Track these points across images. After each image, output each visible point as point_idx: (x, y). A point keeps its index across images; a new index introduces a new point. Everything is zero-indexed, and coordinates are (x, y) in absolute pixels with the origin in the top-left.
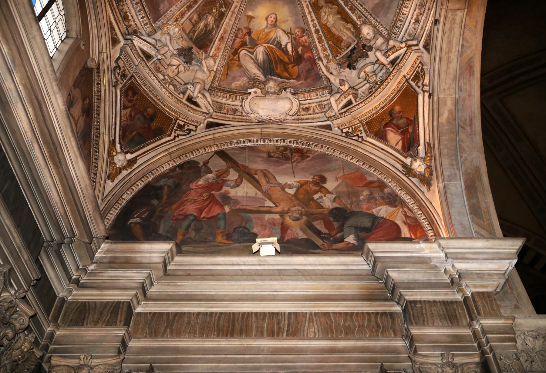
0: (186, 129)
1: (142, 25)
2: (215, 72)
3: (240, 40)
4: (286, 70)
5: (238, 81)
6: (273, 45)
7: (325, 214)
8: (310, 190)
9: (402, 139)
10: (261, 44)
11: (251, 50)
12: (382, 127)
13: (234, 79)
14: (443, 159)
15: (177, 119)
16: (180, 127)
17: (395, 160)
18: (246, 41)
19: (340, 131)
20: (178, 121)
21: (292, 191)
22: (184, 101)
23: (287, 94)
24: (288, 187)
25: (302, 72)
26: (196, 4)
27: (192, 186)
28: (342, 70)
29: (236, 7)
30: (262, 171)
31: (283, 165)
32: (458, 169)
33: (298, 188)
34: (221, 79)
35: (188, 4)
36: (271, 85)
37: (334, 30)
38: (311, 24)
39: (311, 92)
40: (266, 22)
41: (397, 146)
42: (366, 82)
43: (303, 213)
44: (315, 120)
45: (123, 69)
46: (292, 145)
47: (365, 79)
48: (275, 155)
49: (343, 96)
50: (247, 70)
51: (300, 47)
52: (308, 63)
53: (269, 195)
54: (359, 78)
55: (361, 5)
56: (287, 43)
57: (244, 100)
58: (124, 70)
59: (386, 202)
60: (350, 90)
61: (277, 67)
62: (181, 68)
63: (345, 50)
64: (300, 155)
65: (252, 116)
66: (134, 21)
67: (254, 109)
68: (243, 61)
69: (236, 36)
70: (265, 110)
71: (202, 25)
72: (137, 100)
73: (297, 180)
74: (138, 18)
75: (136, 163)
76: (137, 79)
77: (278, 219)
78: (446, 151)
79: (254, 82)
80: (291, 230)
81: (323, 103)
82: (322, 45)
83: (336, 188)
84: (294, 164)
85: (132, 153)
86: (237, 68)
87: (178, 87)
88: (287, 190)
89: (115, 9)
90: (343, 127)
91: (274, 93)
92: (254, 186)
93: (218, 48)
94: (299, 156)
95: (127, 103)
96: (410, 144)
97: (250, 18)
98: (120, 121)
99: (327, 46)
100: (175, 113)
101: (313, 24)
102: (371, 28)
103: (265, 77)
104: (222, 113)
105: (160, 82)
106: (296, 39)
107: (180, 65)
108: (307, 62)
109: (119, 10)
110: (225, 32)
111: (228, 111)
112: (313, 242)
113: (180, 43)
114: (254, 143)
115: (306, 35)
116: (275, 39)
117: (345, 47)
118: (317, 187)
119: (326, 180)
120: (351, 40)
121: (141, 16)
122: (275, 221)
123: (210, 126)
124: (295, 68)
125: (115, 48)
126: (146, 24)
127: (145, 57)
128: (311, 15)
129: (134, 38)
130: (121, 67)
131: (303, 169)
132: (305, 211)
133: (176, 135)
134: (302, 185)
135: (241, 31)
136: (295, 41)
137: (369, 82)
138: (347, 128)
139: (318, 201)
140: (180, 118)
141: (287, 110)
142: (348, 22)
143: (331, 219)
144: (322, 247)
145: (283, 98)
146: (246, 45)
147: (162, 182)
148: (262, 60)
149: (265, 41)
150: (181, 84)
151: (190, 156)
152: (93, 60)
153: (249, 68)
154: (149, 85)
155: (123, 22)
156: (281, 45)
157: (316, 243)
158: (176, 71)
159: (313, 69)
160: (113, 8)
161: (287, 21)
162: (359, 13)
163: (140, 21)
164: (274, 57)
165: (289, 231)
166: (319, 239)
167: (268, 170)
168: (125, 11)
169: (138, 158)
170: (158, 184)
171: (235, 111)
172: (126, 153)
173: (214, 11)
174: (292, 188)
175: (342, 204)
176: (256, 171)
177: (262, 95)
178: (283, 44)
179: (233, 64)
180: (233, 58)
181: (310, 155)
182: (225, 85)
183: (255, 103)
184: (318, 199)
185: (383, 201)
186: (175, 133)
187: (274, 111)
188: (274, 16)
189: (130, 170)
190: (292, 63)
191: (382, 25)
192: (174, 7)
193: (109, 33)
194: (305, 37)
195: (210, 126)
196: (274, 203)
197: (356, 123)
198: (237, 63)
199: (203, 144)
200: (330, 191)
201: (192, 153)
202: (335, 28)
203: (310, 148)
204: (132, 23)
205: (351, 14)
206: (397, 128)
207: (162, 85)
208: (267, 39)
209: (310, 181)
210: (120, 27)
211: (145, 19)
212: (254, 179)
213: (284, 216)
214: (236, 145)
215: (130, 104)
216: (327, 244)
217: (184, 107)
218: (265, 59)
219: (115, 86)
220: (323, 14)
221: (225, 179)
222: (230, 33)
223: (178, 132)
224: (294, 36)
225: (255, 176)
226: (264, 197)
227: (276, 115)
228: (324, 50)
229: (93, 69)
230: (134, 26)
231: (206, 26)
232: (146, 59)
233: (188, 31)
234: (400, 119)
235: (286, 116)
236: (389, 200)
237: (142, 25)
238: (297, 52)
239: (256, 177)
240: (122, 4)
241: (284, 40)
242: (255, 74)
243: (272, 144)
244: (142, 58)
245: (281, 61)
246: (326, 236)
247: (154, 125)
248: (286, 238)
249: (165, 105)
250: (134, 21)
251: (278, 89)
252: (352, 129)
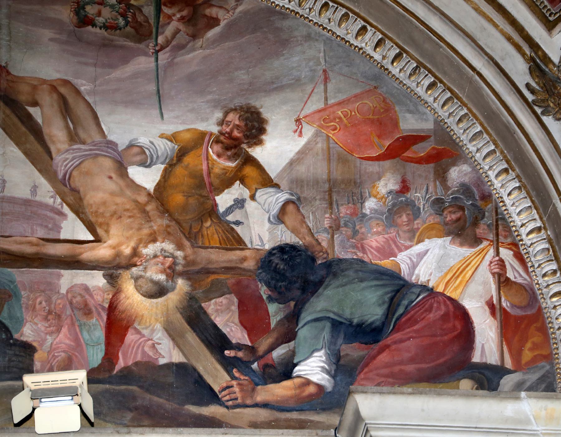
7: (244, 270)
8: (209, 173)
24: (138, 158)
30: (53, 88)
31: (125, 61)
43: (179, 268)
48: (99, 14)
53: (75, 191)
64: (184, 13)
73: (170, 128)
77: (99, 288)
80: (138, 332)
83: (292, 163)
84: (163, 57)
92: (27, 154)
94: (182, 18)
112: (200, 377)
118: (229, 158)
119: (262, 131)
122: (91, 296)
131: (191, 79)
132: (185, 258)
139: (230, 218)
143: (264, 291)
144: (224, 396)
157: (210, 380)
165: (130, 337)
166: (219, 367)
167: (75, 81)
174: (149, 166)
175: (304, 230)
176: (35, 87)
181: (221, 14)
184: (230, 210)
185: (438, 219)
196: (91, 228)
200: (273, 175)
209: (211, 134)
212: (28, 120)
213: (117, 277)
216: (239, 384)
225: (32, 110)
226: (59, 200)
236: (458, 215)
246: (240, 354)
248: (121, 364)
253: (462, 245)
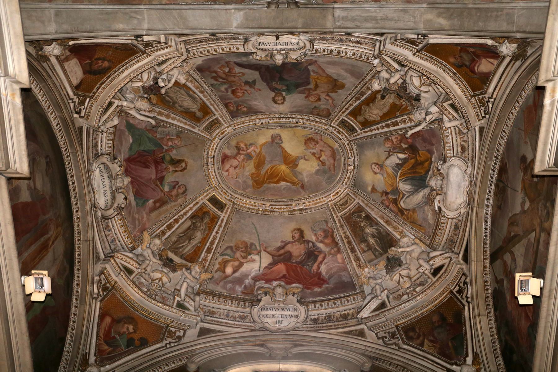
0: (463, 286)
1: (355, 303)
2: (416, 237)
3: (391, 204)
4: (422, 163)
5: (427, 216)
6: (398, 172)
9: (485, 58)
10: (396, 184)
11: (401, 195)
12: (475, 76)
13: (425, 220)
15: (451, 292)
16: (460, 292)
17: (512, 67)
18: (392, 198)
20: (454, 291)
21: (527, 205)
22: (434, 280)
23: (443, 168)
25: (425, 147)
26: (352, 242)
27: (509, 309)
28: (423, 106)
29: (363, 201)
32: (502, 9)
33: (526, 194)
34: (424, 233)
35: (349, 251)
36: (434, 183)
37: (385, 110)
38: (381, 131)
40: (378, 175)
41: (494, 63)
44: (474, 142)
45: (387, 333)
46: (495, 176)
49: (445, 112)
50: (419, 204)
51: (401, 146)
52: (417, 140)
54: (429, 91)
55: (356, 87)
56: (398, 157)
57: (446, 215)
58: (389, 333)
60: (438, 105)
61: (419, 173)
62: (404, 273)
65: (463, 211)
66: (350, 309)
67: (455, 207)
68: (410, 206)
69: (388, 207)
70: (458, 196)
71: (371, 241)
72: (420, 329)
73: (520, 191)
74: (348, 305)
75: (478, 355)
76: (400, 322)
78: (481, 24)
79: (429, 200)
82: (400, 122)
85: (467, 356)
86: (416, 214)
87: (423, 280)
88: (526, 208)
89: (335, 325)
90: (480, 116)
91: (442, 180)
92: (518, 243)
93: (395, 228)
95: (418, 341)
97: (374, 190)
98: (432, 355)
99: (400, 119)
100: (445, 292)
101: (381, 129)
102: (374, 80)
103: (427, 187)
104: (457, 241)
105: (408, 301)
106: (394, 147)
107: (400, 274)
108: (416, 141)
109: (337, 322)
110: (383, 218)
111: (456, 235)
113: (382, 267)
114: (488, 218)
115: (391, 137)
116: (394, 169)
121: (346, 302)
123: (466, 259)
124: (420, 154)
125: (367, 335)
126: (354, 299)
127: (382, 309)
128: (373, 130)
129: (360, 317)
130: (384, 335)
133: (465, 299)
134: (524, 188)
135: (383, 202)
136: (396, 149)
138: (480, 111)
140: (452, 289)
141: (460, 171)
142: (376, 98)
145: (448, 174)
146: (396, 199)
147: (503, 338)
148: (411, 187)
149: (394, 179)
150: (421, 276)
151: (489, 293)
152: (363, 365)
153: (417, 202)
154: (410, 313)
155: (347, 320)
156: (399, 164)
158: (405, 279)
159: (423, 135)
160: (333, 327)
161: (378, 154)
162: (364, 88)
163: (351, 304)
164: (410, 173)
168: (339, 316)
169: (475, 350)
170: (504, 343)
171: (457, 227)
172: (465, 361)
173: (362, 225)
177: (443, 195)
178: (398, 161)
179: (411, 216)
180: (406, 215)
182: (430, 231)
183: (450, 205)
186: (463, 299)
187: (459, 187)
188: (373, 166)
189: (482, 366)
190: (416, 156)
191: (371, 70)
192: (348, 266)
193: (352, 338)
194: (393, 138)
195: (466, 259)
196: (533, 231)
197: (474, 101)
198: (411, 213)
199: (479, 275)
201: (487, 290)
202: (383, 109)
203: (499, 157)
204: (351, 311)
205: (367, 95)
206: (473, 61)
207: (412, 299)
208: (393, 176)
210: (350, 324)
211: (349, 299)
214: (488, 239)
215: (421, 338)
217: (440, 281)
218: (410, 183)
219: (400, 348)
220: (371, 118)
221: (509, 270)
222: (383, 213)
223: (464, 297)
224: (392, 149)
227: (465, 184)
228: (404, 121)
229: (373, 365)
230: (353, 310)
231: (373, 236)
232: (383, 308)
233: (373, 257)
235: (466, 174)
237: (355, 303)
238: (406, 148)
239: (513, 234)
240: (332, 317)
241: (394, 159)
242: (423, 197)
243: (491, 199)
244: (380, 313)
245: (413, 167)
247: (450, 319)
249: (427, 306)
250: (350, 309)
251: (439, 178)
252: (481, 106)
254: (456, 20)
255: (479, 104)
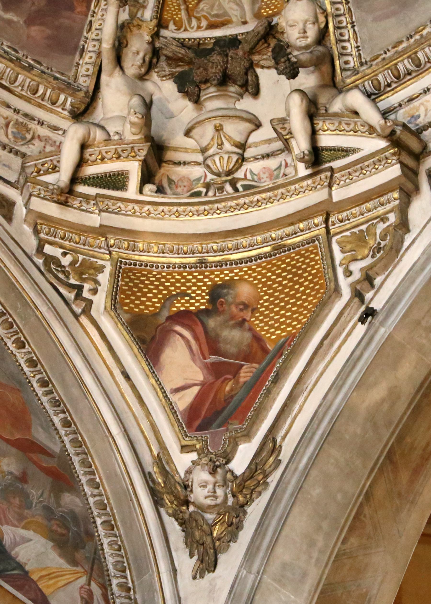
9: (203, 384)
12: (165, 314)
14: (296, 510)
19: (34, 242)
39: (24, 68)
42: (200, 158)
47: (203, 150)
59: (52, 531)
63: (199, 27)
81: (33, 125)
96: (218, 413)
117: (205, 17)
120: (238, 13)
137: (209, 162)
138: (61, 247)
185: (45, 522)
234: (234, 327)
236: (64, 532)
253: (61, 556)
254: (359, 431)
255: (81, 257)
